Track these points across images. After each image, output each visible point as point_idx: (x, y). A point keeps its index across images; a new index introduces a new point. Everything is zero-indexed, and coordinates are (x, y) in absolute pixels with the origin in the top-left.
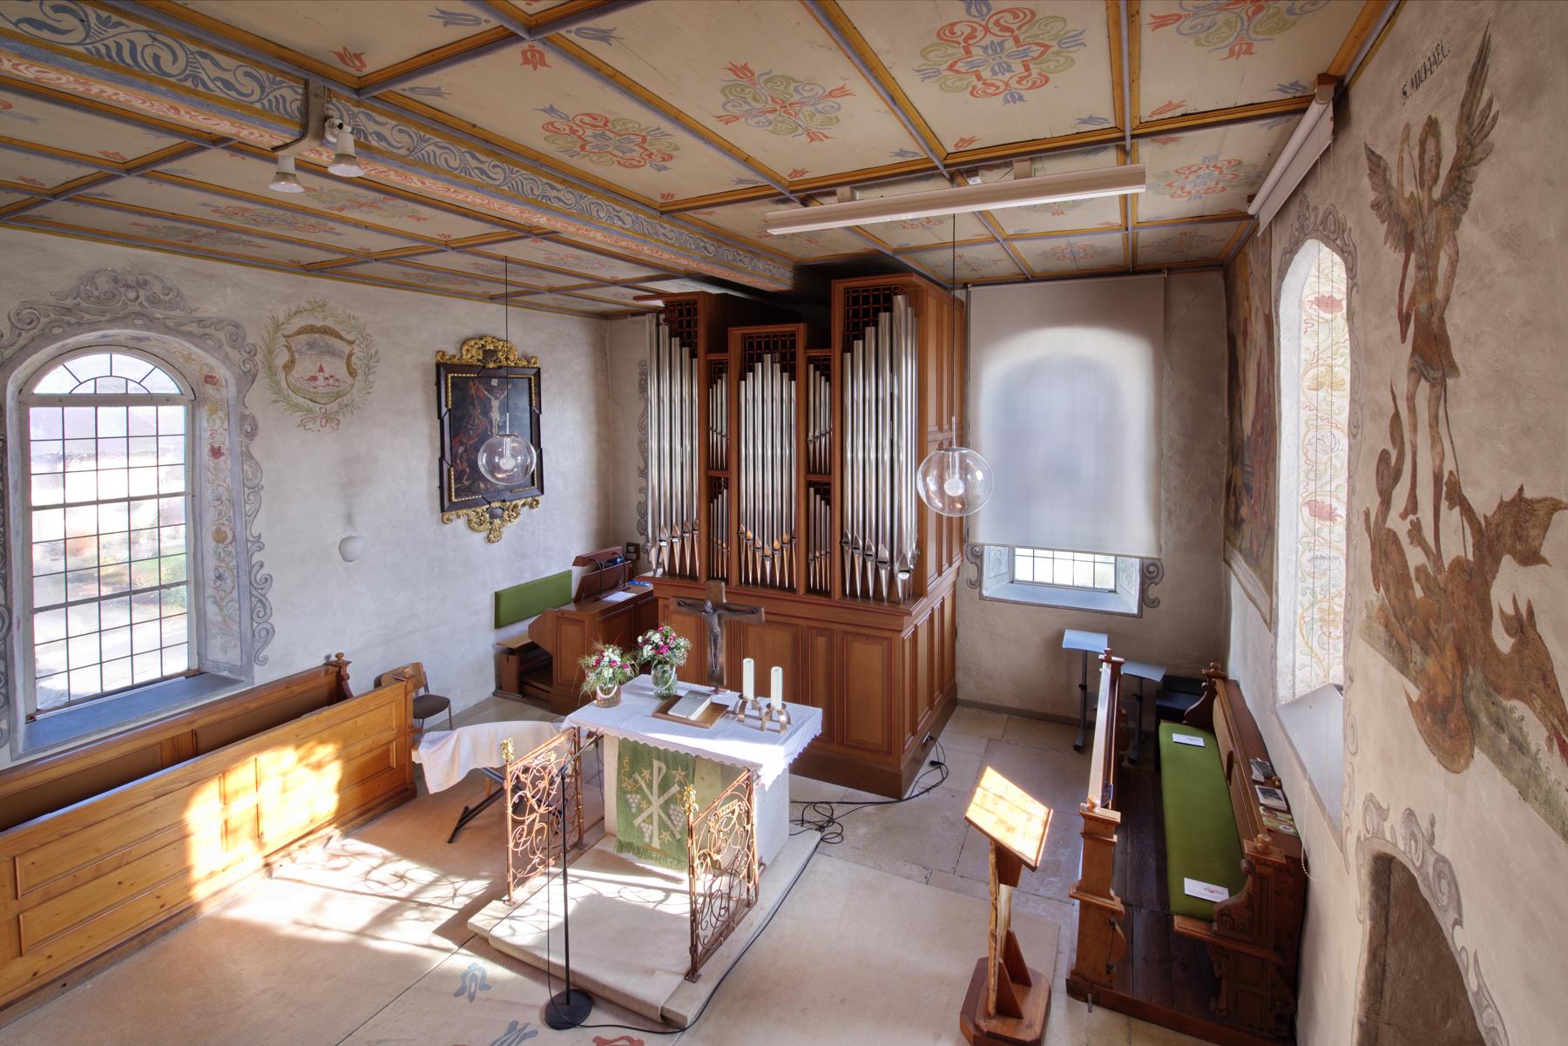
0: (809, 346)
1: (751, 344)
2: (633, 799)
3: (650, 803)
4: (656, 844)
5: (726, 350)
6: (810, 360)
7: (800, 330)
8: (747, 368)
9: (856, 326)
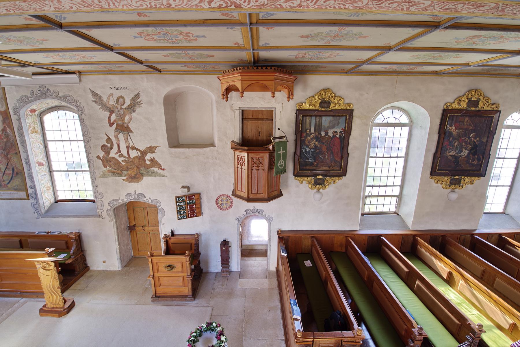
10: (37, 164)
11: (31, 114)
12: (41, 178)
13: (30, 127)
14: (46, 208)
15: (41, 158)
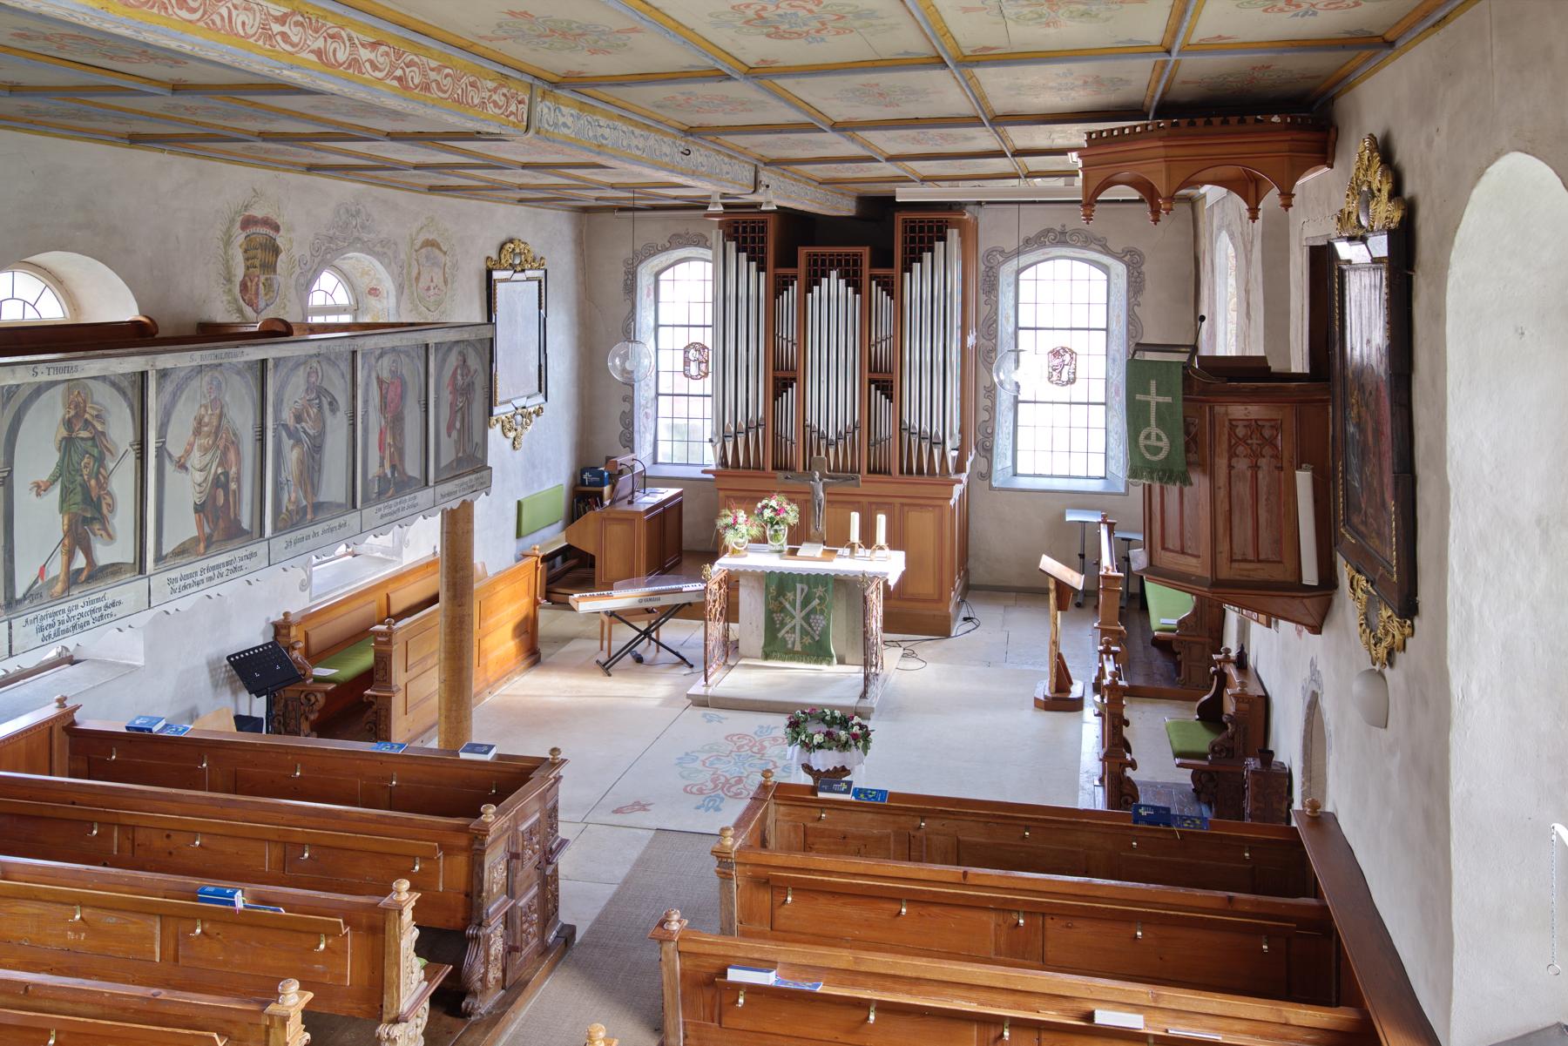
0: (872, 266)
1: (815, 262)
2: (777, 617)
3: (793, 617)
4: (798, 647)
5: (796, 266)
6: (872, 278)
7: (866, 252)
8: (813, 281)
9: (912, 251)
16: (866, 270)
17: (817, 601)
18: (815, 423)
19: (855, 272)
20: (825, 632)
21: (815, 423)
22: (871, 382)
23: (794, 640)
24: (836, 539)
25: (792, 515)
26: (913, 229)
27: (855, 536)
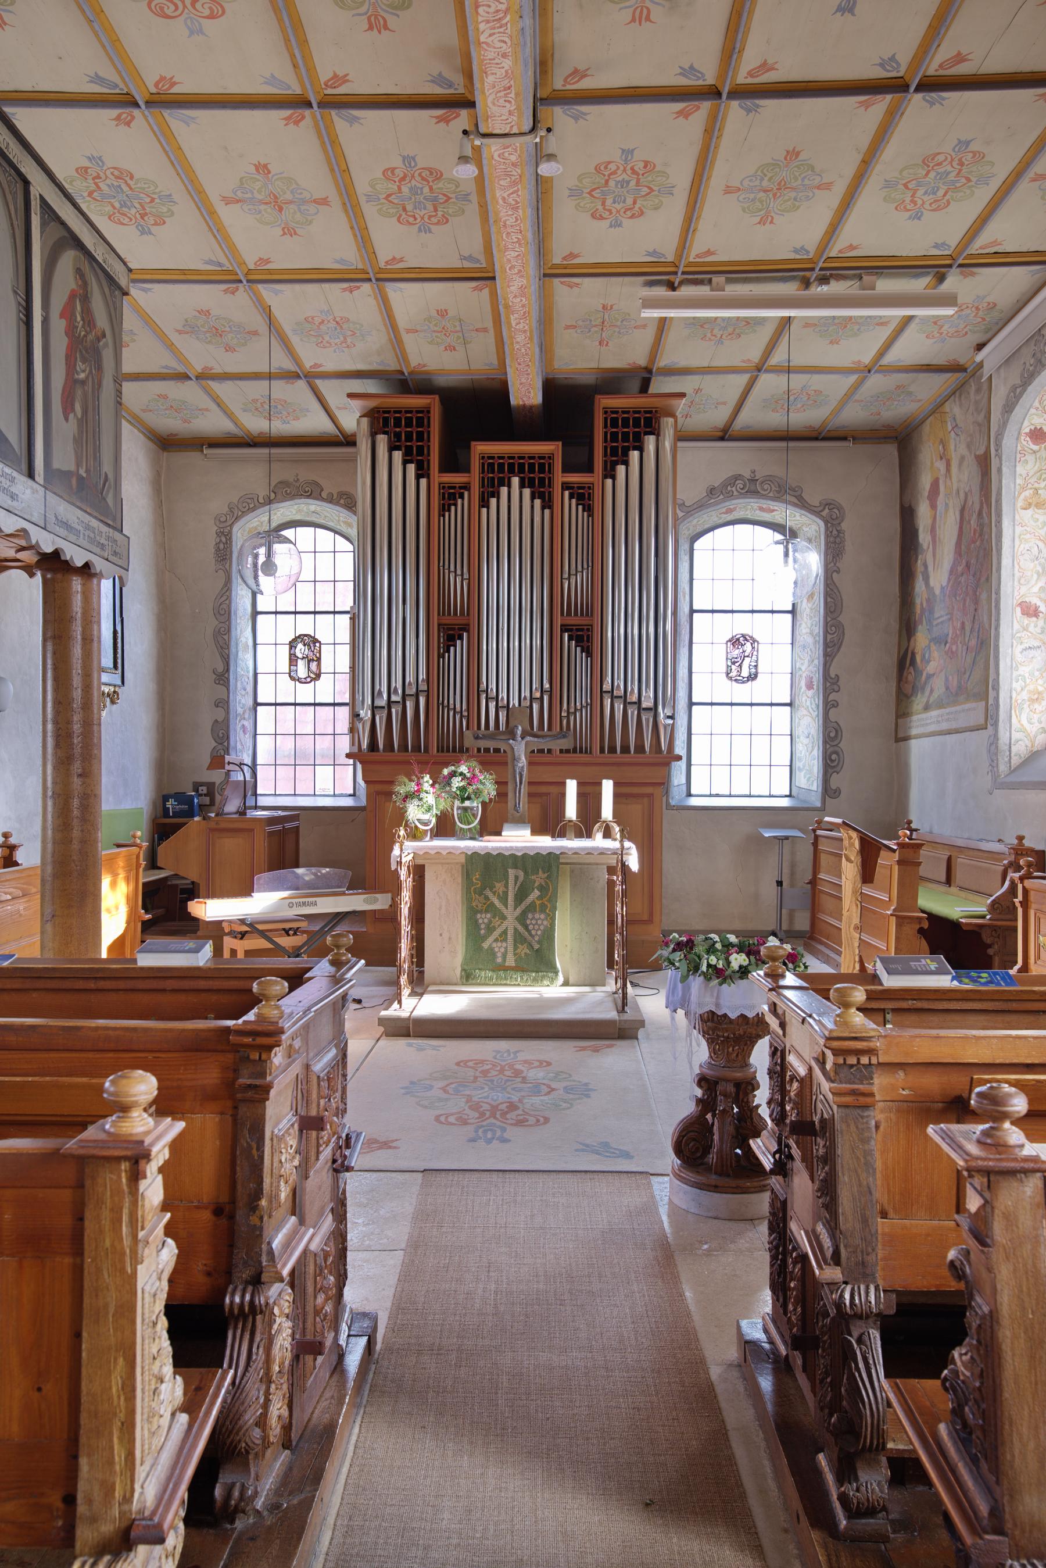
1: (491, 465)
2: (483, 919)
3: (504, 918)
4: (511, 961)
5: (467, 470)
9: (614, 451)
10: (1018, 610)
11: (1035, 448)
12: (1019, 657)
13: (1024, 488)
14: (1015, 761)
15: (1036, 589)
16: (560, 477)
17: (537, 893)
18: (493, 686)
19: (542, 481)
20: (549, 936)
21: (493, 686)
22: (564, 628)
23: (506, 951)
24: (549, 822)
25: (489, 788)
26: (614, 423)
27: (571, 811)
